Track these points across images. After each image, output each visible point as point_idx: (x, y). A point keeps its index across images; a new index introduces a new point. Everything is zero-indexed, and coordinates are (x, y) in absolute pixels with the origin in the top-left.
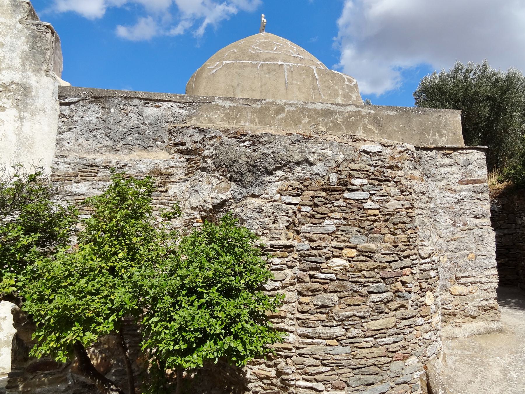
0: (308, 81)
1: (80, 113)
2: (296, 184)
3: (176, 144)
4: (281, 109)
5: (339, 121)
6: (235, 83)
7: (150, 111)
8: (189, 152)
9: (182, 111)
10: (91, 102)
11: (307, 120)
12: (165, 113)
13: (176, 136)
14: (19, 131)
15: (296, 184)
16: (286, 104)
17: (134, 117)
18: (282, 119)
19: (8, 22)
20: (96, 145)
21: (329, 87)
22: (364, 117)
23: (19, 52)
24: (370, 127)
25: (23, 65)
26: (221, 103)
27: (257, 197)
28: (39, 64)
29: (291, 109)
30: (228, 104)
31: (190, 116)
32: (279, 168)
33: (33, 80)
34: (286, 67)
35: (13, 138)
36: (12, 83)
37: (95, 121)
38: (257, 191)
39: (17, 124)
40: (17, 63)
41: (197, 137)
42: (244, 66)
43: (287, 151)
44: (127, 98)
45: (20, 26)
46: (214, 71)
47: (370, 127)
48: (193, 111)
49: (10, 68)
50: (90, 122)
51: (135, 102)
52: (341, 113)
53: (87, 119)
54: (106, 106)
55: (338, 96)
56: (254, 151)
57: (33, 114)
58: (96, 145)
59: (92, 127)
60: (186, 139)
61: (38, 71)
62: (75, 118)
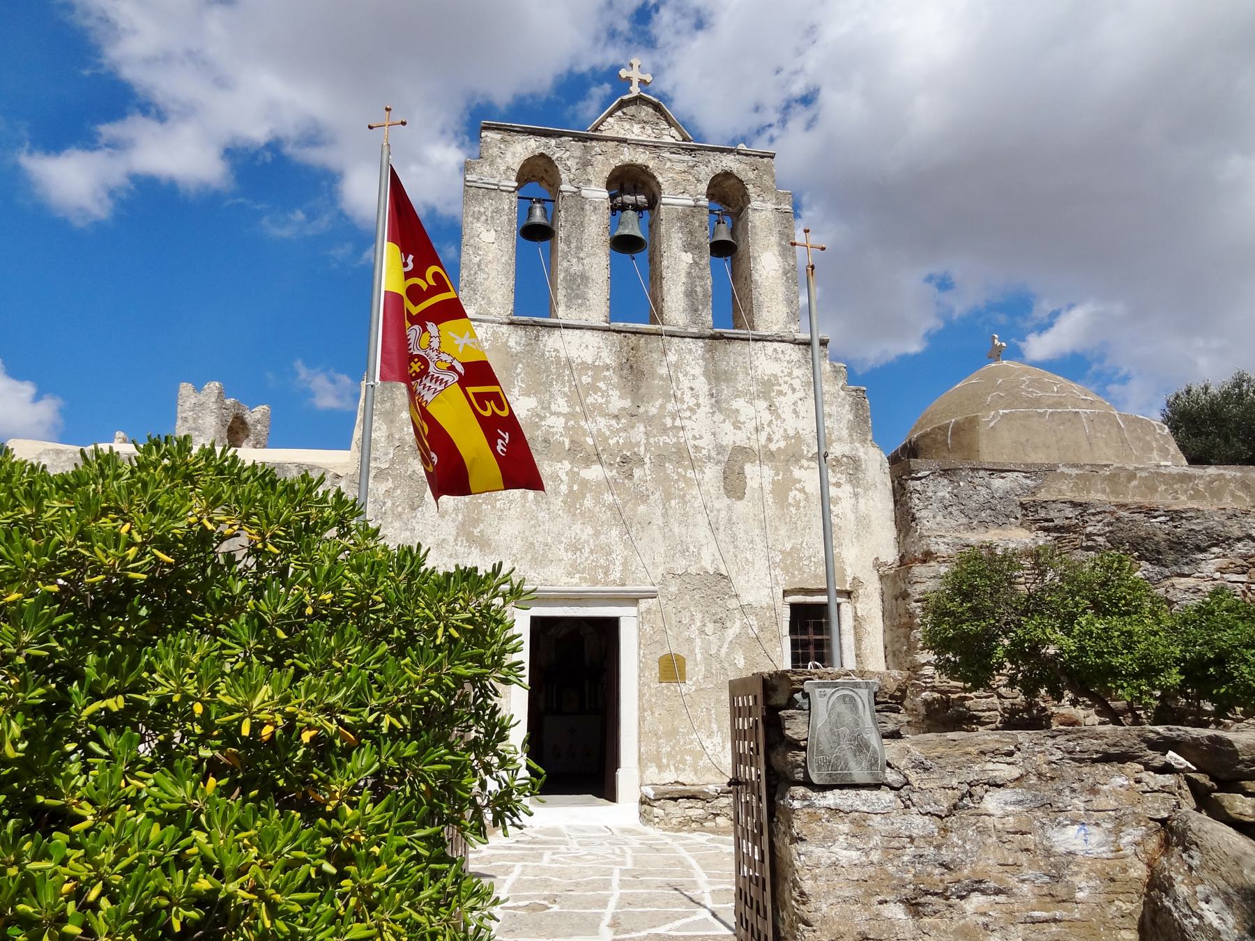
0: (1114, 431)
1: (932, 488)
2: (1240, 562)
3: (1036, 521)
4: (1132, 476)
5: (1201, 487)
6: (1023, 439)
7: (997, 483)
8: (1057, 529)
9: (1028, 481)
10: (941, 475)
11: (1163, 487)
12: (1013, 485)
13: (1036, 511)
14: (855, 509)
15: (1240, 562)
16: (1137, 469)
17: (983, 491)
18: (1135, 487)
19: (833, 390)
20: (954, 523)
21: (1140, 439)
22: (1230, 481)
23: (845, 421)
24: (1239, 493)
25: (851, 435)
26: (1066, 470)
27: (1188, 576)
28: (865, 434)
29: (1144, 474)
30: (1074, 472)
31: (1037, 487)
32: (1214, 545)
33: (861, 453)
34: (1083, 416)
35: (851, 517)
36: (844, 456)
37: (948, 496)
38: (1186, 570)
39: (853, 501)
40: (845, 433)
41: (1069, 512)
42: (1029, 416)
43: (1224, 526)
44: (973, 470)
45: (842, 393)
46: (992, 424)
47: (1239, 493)
48: (1039, 481)
49: (839, 439)
50: (944, 497)
51: (982, 473)
52: (1201, 477)
53: (939, 494)
54: (954, 479)
55: (1152, 449)
56: (1176, 527)
57: (866, 490)
58: (954, 523)
59: (946, 503)
60: (1052, 514)
61: (864, 441)
62: (930, 494)
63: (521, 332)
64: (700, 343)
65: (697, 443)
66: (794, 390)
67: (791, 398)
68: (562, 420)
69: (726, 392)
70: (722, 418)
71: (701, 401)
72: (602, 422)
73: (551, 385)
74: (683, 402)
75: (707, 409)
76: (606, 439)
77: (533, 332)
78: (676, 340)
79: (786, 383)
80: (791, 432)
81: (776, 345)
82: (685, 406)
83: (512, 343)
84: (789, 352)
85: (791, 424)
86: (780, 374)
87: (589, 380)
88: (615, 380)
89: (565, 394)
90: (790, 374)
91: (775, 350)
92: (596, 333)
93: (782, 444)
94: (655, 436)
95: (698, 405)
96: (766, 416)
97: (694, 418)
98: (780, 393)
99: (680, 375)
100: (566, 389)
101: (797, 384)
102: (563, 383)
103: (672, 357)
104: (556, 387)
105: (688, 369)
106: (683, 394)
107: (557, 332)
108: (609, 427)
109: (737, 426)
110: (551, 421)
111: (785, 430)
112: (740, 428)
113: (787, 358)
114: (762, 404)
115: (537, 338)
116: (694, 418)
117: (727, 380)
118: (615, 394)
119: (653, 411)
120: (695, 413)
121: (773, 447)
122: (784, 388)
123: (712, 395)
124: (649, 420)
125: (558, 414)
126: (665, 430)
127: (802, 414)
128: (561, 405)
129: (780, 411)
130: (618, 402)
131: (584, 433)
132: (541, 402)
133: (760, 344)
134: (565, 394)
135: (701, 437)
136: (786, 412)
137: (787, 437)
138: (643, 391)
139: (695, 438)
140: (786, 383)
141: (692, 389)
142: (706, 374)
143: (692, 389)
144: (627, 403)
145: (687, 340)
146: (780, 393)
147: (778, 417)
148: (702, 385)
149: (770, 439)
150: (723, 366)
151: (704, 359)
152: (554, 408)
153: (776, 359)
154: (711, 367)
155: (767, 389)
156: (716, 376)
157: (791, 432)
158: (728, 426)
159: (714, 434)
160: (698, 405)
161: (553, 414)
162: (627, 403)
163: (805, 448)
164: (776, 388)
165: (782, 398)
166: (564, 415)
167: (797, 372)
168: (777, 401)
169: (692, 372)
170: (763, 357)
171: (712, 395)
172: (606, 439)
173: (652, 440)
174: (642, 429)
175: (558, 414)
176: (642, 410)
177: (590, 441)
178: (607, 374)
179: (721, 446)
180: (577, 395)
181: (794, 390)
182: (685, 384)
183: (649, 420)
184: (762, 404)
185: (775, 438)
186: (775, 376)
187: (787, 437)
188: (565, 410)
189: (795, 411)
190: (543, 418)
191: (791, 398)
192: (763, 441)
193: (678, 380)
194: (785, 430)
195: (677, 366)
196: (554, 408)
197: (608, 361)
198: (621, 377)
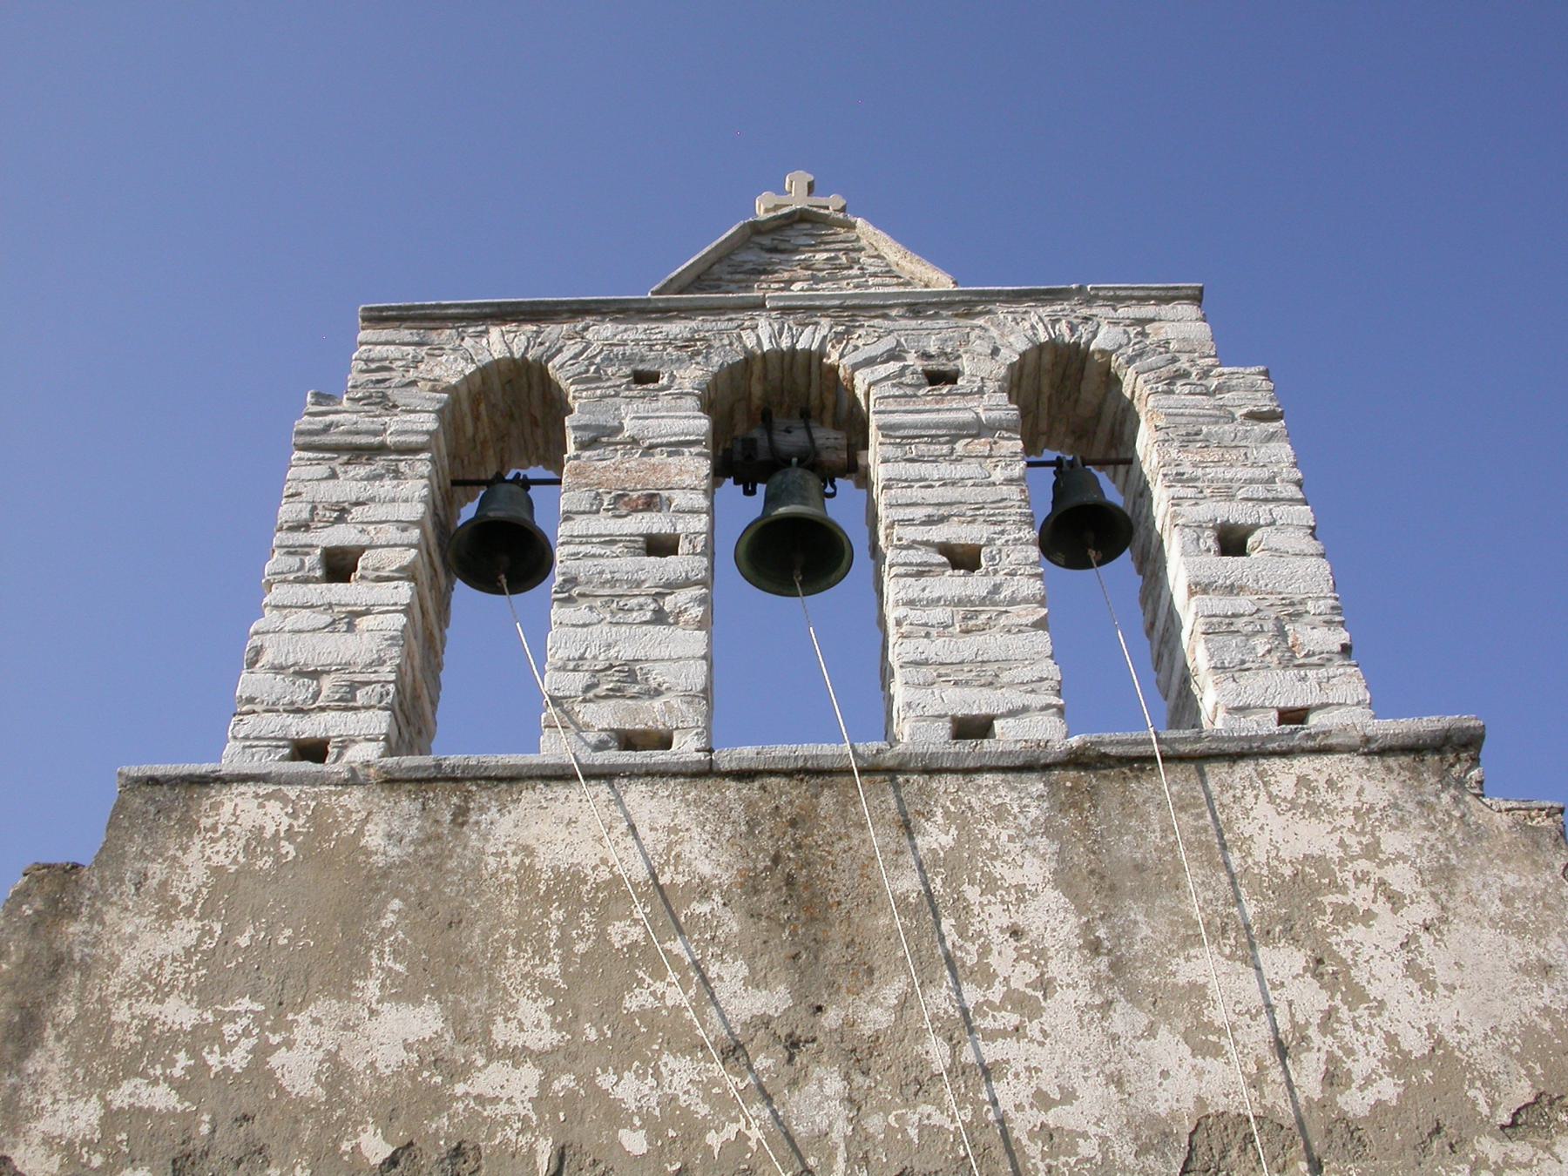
63: (407, 805)
64: (1036, 785)
65: (1051, 1118)
66: (1395, 901)
67: (1388, 928)
68: (530, 1075)
69: (1146, 928)
70: (1143, 1020)
71: (1055, 969)
72: (680, 1073)
73: (499, 957)
74: (985, 976)
75: (1083, 996)
76: (694, 1130)
77: (444, 805)
78: (950, 783)
79: (1362, 878)
80: (1415, 1044)
81: (1303, 765)
82: (996, 993)
83: (374, 838)
84: (1355, 781)
85: (1409, 1016)
86: (1335, 853)
87: (636, 933)
88: (732, 924)
89: (547, 987)
90: (1372, 851)
91: (1302, 781)
92: (663, 788)
93: (1388, 1089)
94: (885, 1108)
95: (1045, 985)
96: (1310, 999)
97: (1033, 1029)
98: (1346, 915)
99: (972, 893)
100: (553, 969)
101: (1400, 877)
102: (542, 953)
103: (935, 837)
104: (516, 965)
105: (999, 869)
106: (985, 951)
107: (531, 796)
108: (706, 1087)
109: (1203, 1040)
110: (490, 1078)
111: (1391, 1039)
112: (1216, 1051)
113: (1351, 801)
114: (1284, 961)
115: (461, 816)
116: (1033, 1029)
117: (1144, 893)
118: (729, 975)
119: (876, 1017)
120: (1035, 1011)
121: (1355, 1103)
122: (1361, 896)
123: (1095, 947)
124: (858, 1055)
125: (516, 1056)
126: (919, 1084)
127: (1442, 975)
128: (531, 1022)
129: (1359, 976)
130: (747, 997)
131: (615, 1115)
132: (457, 1019)
133: (1245, 769)
134: (547, 987)
135: (1068, 1096)
136: (1383, 976)
137: (1400, 1064)
138: (834, 953)
139: (1042, 1100)
140: (1362, 878)
141: (1016, 933)
142: (1064, 879)
143: (1016, 933)
144: (775, 1000)
145: (988, 779)
146: (1346, 915)
147: (1356, 995)
148: (1053, 917)
149: (1333, 1078)
150: (1125, 848)
151: (1050, 830)
152: (502, 1033)
153: (1315, 810)
154: (1079, 855)
155: (1299, 905)
156: (1096, 883)
157: (1415, 1044)
158: (1169, 1047)
159: (1117, 1080)
160: (1045, 985)
161: (492, 1055)
162: (775, 1000)
163: (1478, 1095)
164: (1329, 899)
165: (1357, 932)
166: (539, 1057)
167: (1392, 842)
168: (1339, 942)
169: (1012, 877)
170: (1263, 809)
171: (1095, 947)
172: (694, 1130)
173: (874, 1124)
174: (834, 1085)
175: (516, 1056)
176: (832, 1018)
177: (635, 1142)
178: (704, 908)
179: (1152, 1120)
180: (593, 983)
181: (1395, 901)
182: (994, 918)
183: (858, 1055)
184: (1284, 961)
185: (1360, 1067)
186: (1319, 861)
187: (1400, 1064)
188: (547, 1038)
189: (1412, 969)
190: (463, 1071)
191: (1388, 928)
192: (1310, 1083)
193: (962, 909)
194: (1391, 1039)
195: (954, 864)
196: (502, 1033)
197: (706, 869)
198: (754, 915)
